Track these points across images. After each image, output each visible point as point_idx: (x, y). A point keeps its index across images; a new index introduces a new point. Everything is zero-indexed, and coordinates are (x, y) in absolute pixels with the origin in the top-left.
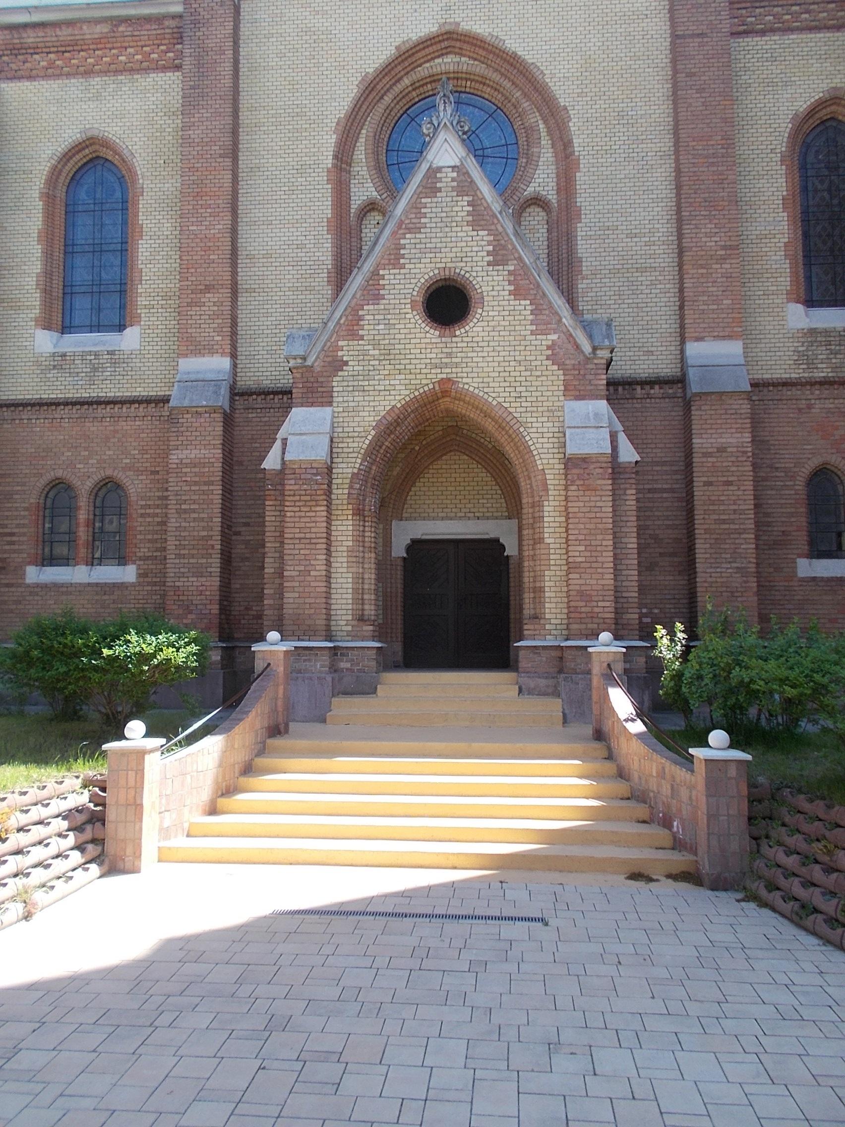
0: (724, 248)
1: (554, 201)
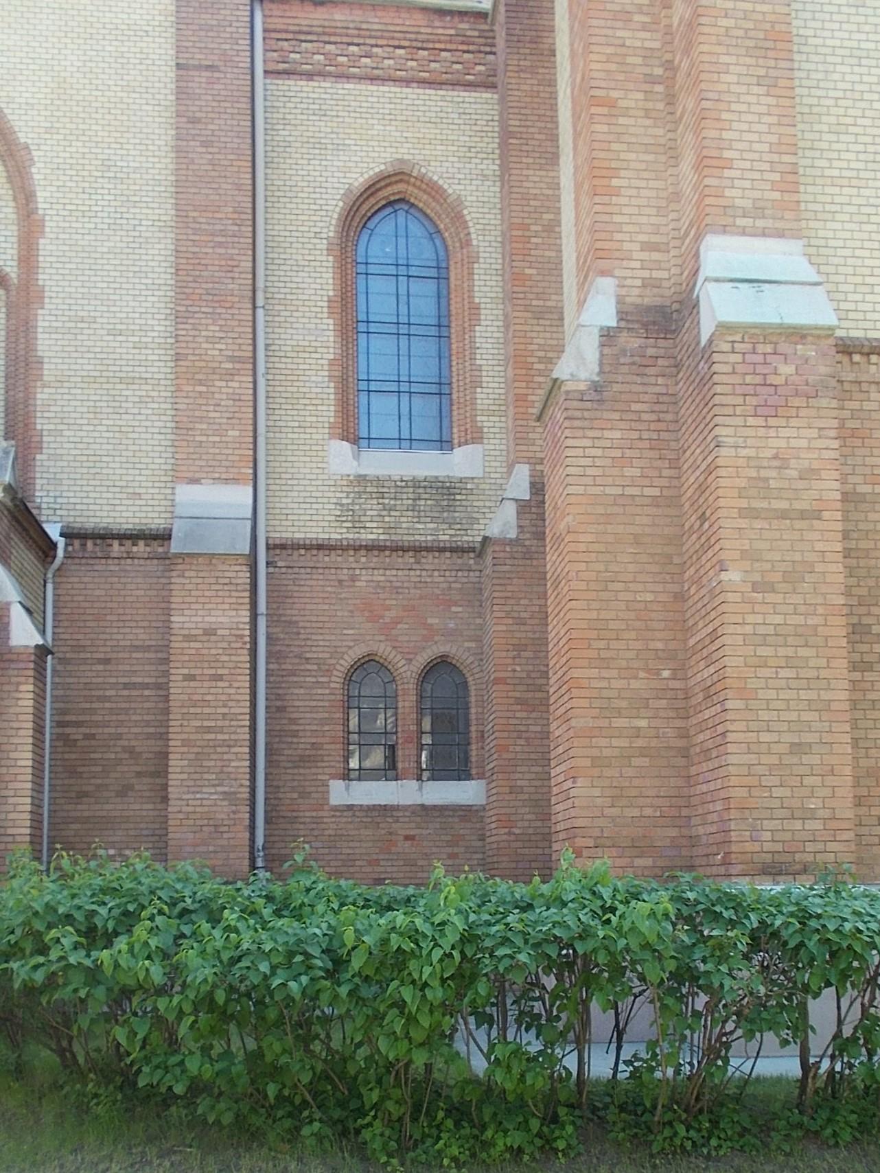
0: (232, 359)
1: (13, 275)
